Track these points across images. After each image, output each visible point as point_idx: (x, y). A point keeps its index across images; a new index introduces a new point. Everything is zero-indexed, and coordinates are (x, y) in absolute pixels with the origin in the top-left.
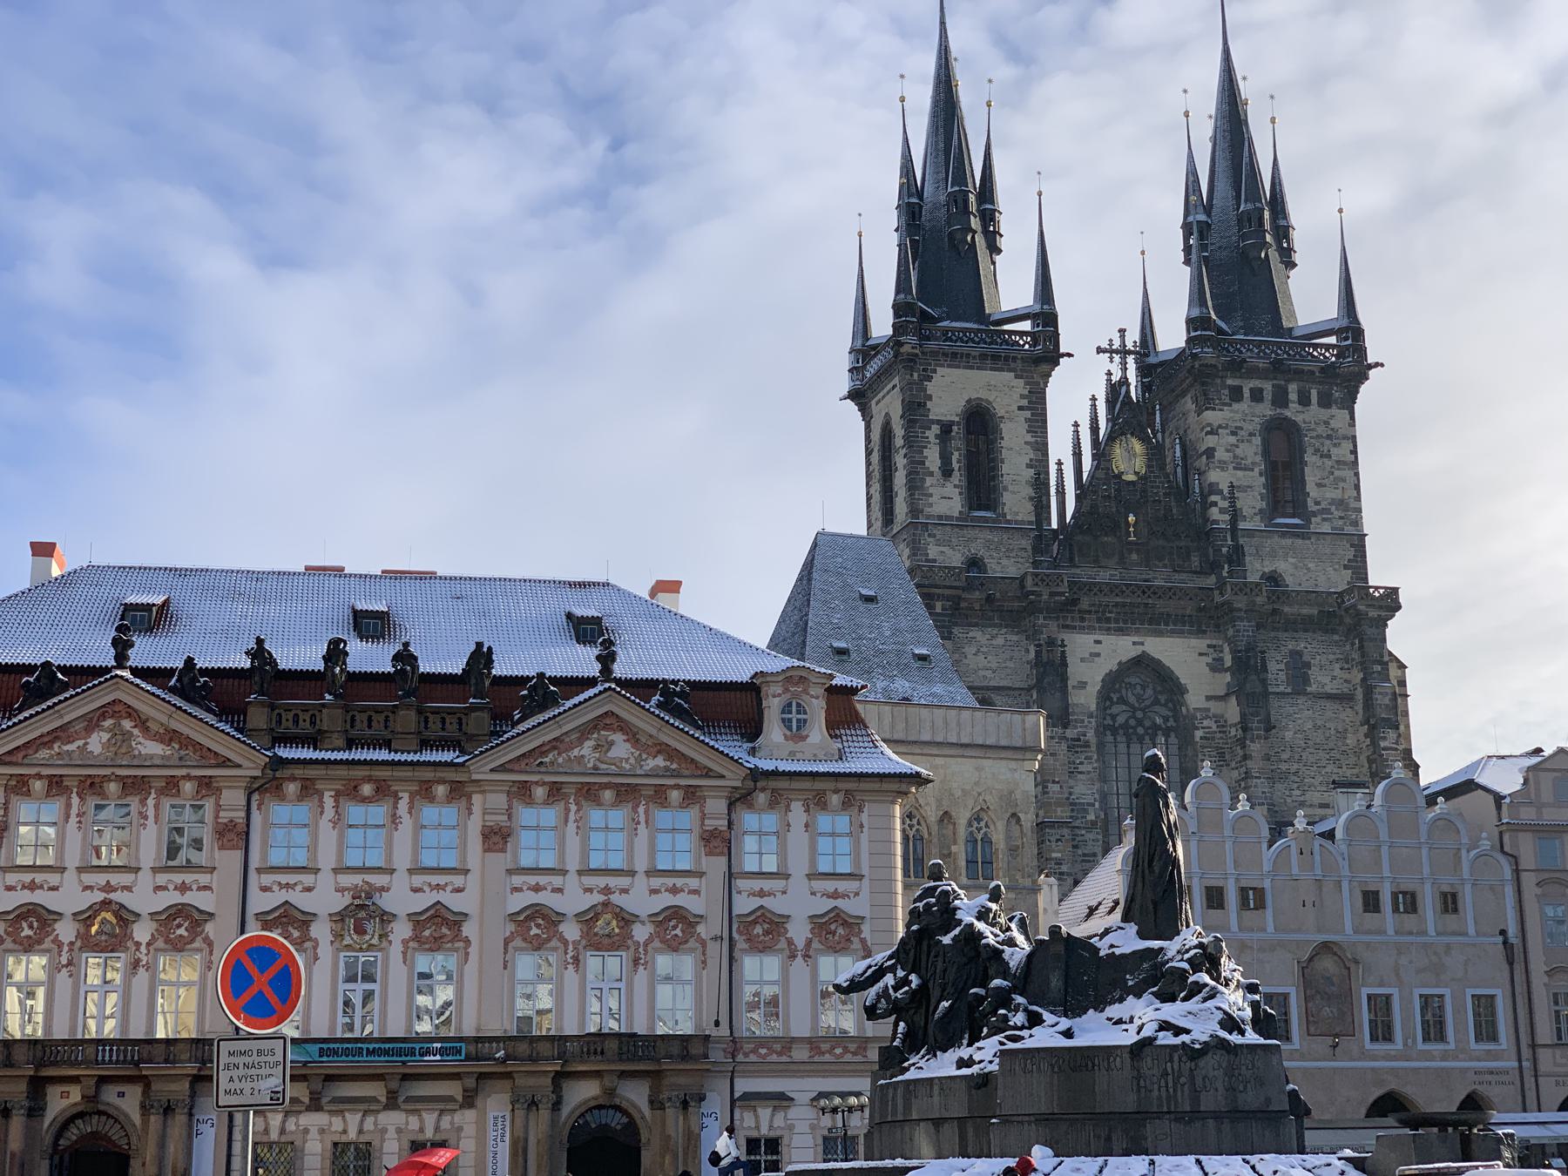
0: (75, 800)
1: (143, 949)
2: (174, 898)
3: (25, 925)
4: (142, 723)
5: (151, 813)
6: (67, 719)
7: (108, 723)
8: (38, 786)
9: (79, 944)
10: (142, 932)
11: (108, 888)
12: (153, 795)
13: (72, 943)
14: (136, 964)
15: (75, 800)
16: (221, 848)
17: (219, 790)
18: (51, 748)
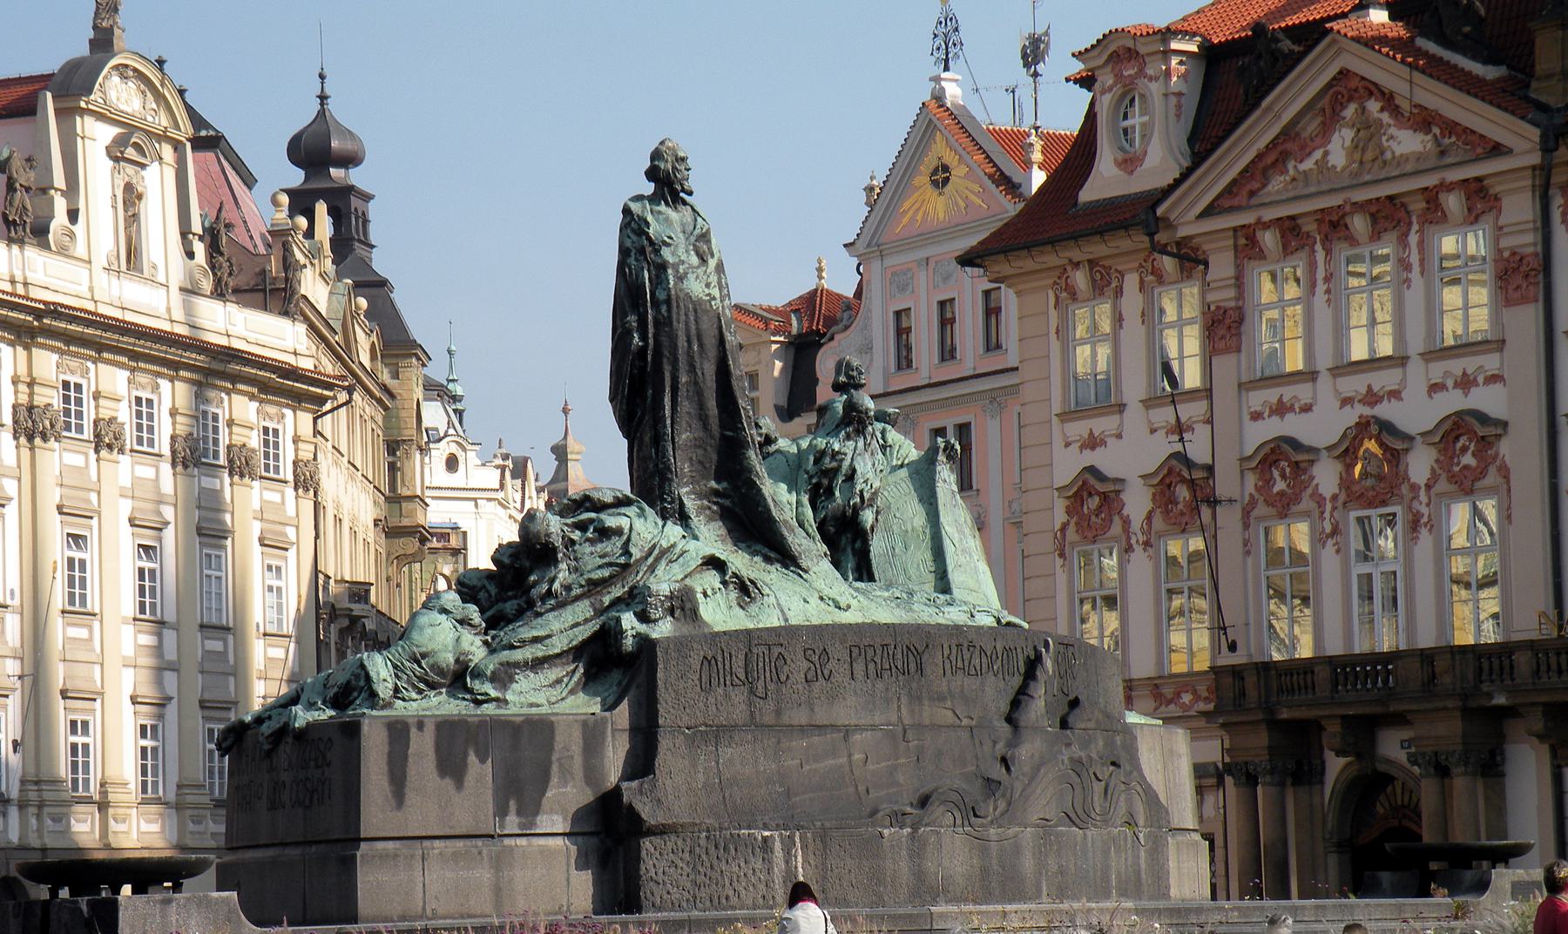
0: (1320, 255)
1: (1422, 493)
2: (1453, 401)
3: (1276, 474)
4: (1389, 101)
5: (1415, 259)
6: (1287, 117)
7: (1350, 111)
8: (1269, 239)
9: (1342, 497)
10: (1420, 465)
11: (1372, 398)
12: (1415, 227)
13: (1335, 498)
14: (1415, 524)
15: (1320, 255)
16: (1509, 303)
17: (1497, 198)
18: (1284, 171)
